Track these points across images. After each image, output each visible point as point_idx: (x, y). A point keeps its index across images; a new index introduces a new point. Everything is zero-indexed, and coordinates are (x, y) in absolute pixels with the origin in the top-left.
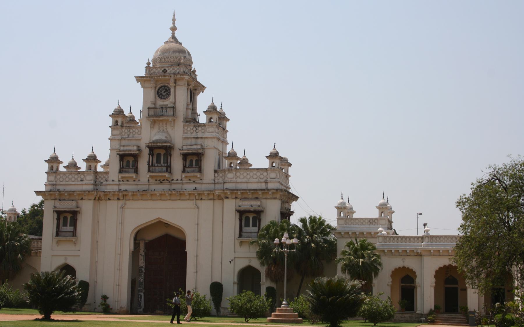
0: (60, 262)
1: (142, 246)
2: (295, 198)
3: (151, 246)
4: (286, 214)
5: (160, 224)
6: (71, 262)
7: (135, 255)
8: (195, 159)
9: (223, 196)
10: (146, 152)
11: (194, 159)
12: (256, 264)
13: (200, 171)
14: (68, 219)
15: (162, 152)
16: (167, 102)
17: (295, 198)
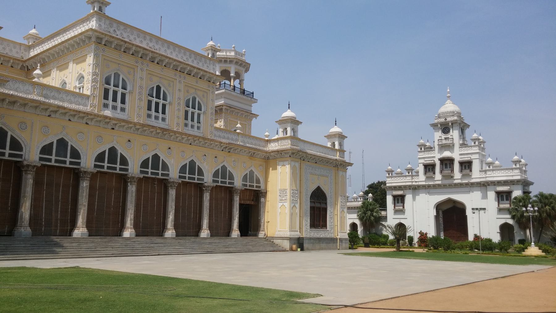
0: (397, 221)
1: (441, 213)
2: (532, 184)
3: (445, 212)
4: (526, 193)
5: (449, 201)
6: (403, 221)
7: (437, 217)
8: (467, 165)
9: (486, 184)
10: (438, 163)
11: (466, 165)
12: (511, 222)
13: (471, 171)
14: (399, 199)
15: (448, 162)
16: (449, 136)
17: (532, 184)
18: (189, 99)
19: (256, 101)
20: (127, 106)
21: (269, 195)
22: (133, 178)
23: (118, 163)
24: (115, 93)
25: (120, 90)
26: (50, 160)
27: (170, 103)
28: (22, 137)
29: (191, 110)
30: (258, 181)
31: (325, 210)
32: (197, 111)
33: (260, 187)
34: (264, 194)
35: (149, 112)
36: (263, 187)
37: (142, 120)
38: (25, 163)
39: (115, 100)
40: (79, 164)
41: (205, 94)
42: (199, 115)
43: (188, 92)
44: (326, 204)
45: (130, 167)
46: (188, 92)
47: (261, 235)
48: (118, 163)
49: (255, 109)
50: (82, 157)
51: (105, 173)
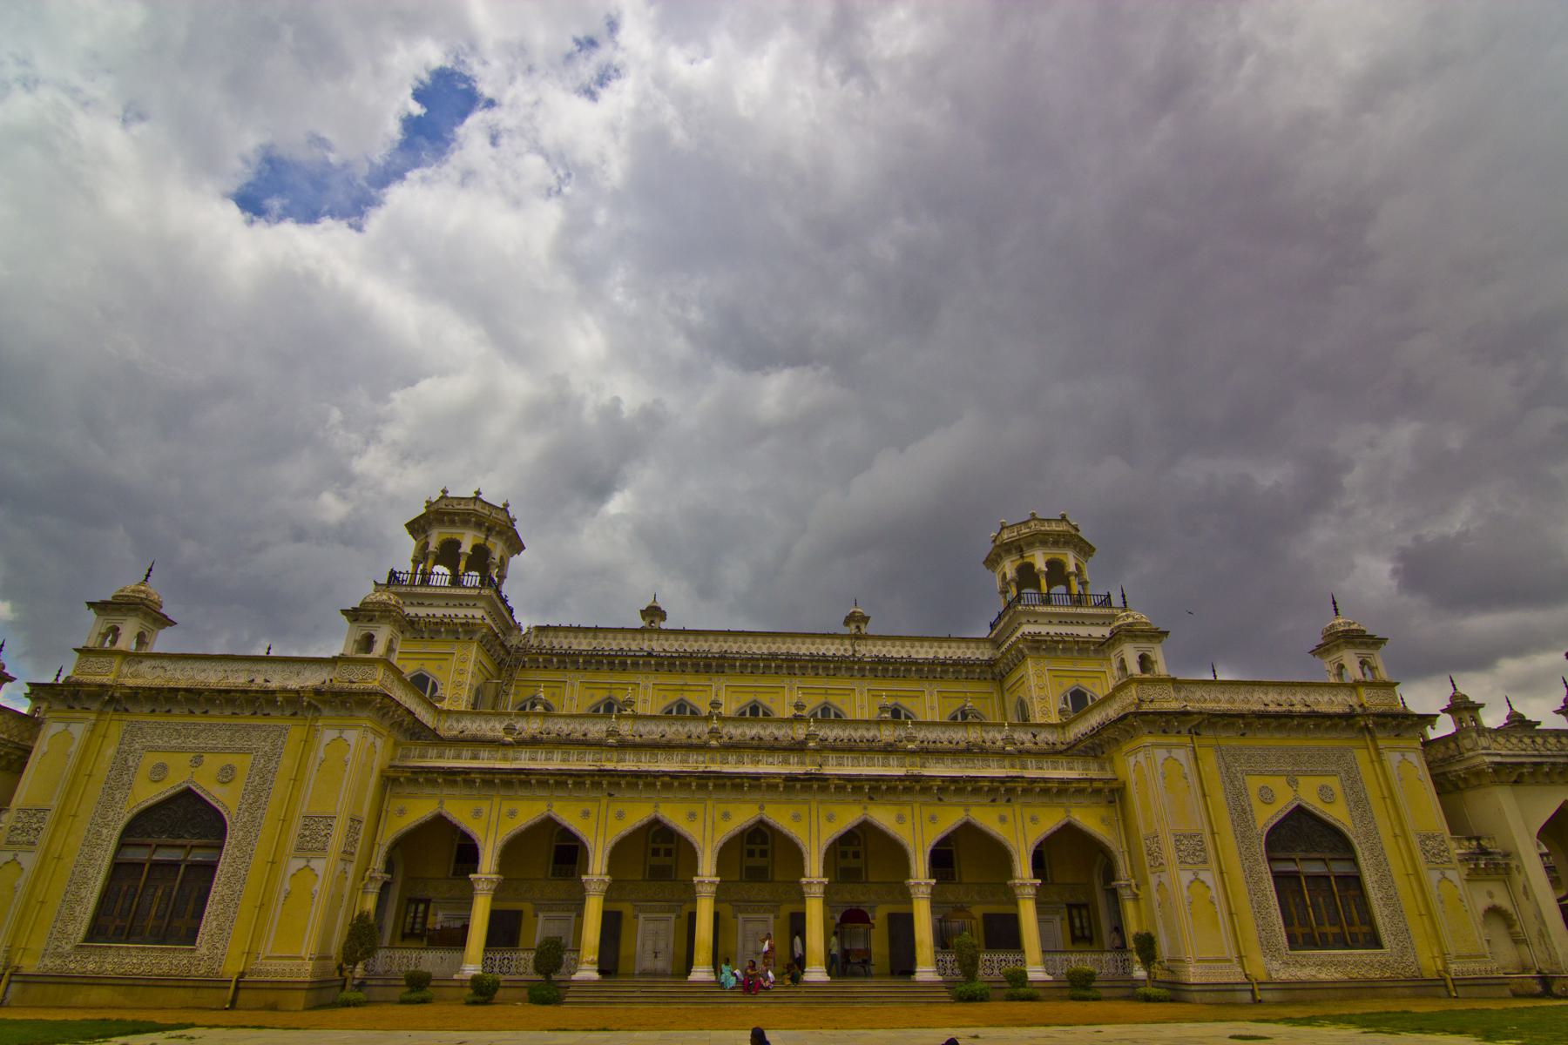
31: (1354, 882)
44: (1353, 860)
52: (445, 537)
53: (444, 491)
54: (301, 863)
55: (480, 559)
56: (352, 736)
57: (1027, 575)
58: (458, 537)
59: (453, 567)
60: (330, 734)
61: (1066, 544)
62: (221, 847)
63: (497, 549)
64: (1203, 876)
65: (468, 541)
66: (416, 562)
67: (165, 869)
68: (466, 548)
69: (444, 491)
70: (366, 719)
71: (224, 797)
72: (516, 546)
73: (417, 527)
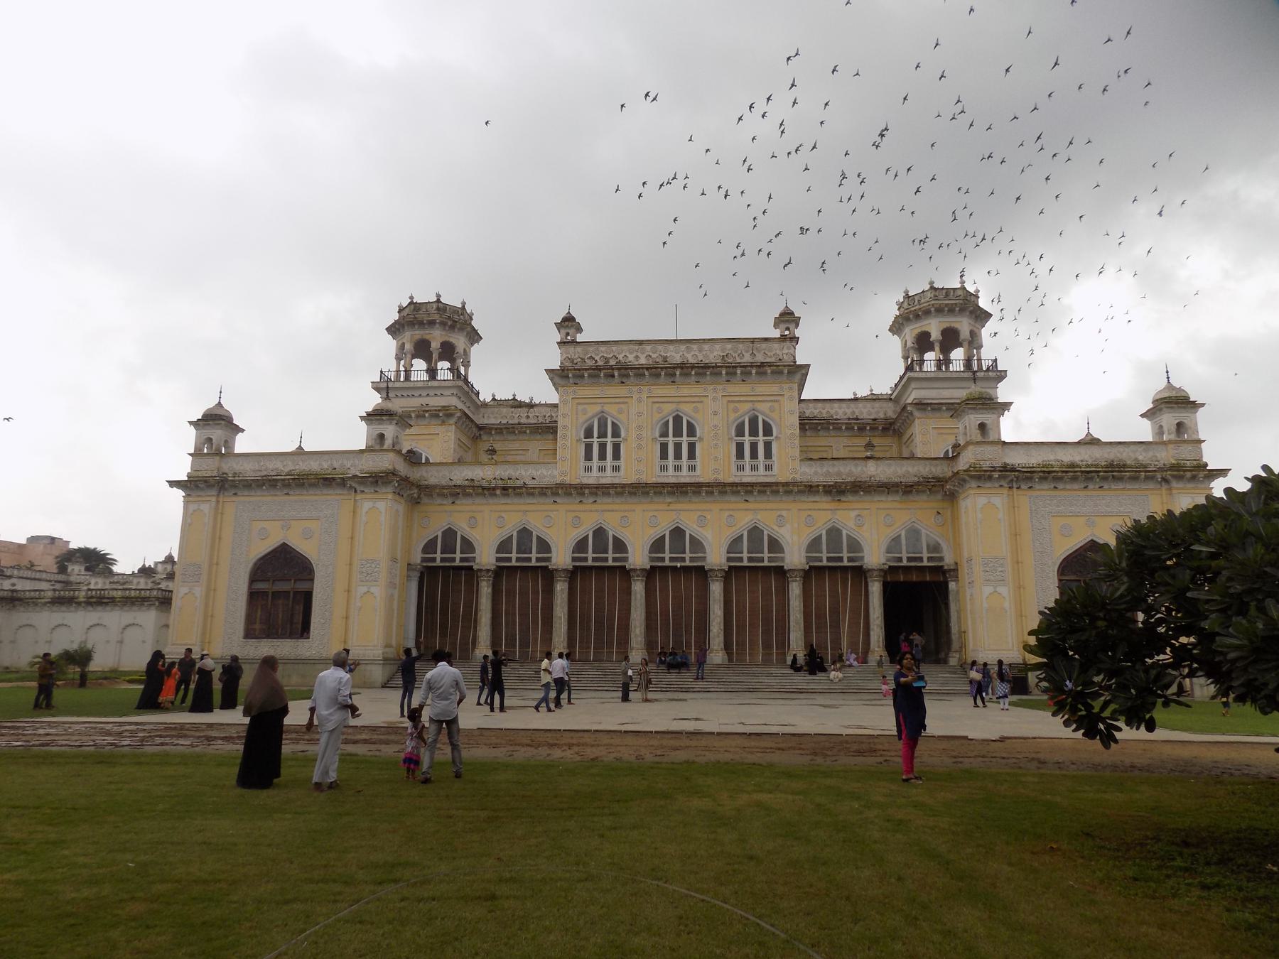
18: (743, 423)
19: (1001, 376)
20: (622, 463)
21: (963, 572)
22: (635, 570)
23: (610, 551)
24: (603, 447)
25: (609, 440)
26: (510, 559)
27: (701, 439)
28: (475, 536)
29: (747, 439)
30: (935, 548)
32: (761, 438)
33: (941, 559)
34: (954, 572)
35: (664, 463)
36: (948, 561)
37: (653, 475)
38: (475, 568)
39: (602, 456)
40: (549, 559)
41: (776, 405)
42: (768, 446)
43: (736, 410)
45: (554, 555)
46: (736, 410)
47: (953, 661)
48: (610, 551)
49: (1003, 392)
50: (553, 549)
51: (591, 568)
52: (418, 337)
53: (411, 298)
54: (364, 589)
55: (448, 351)
56: (381, 505)
57: (923, 343)
58: (427, 337)
59: (428, 359)
60: (367, 505)
61: (962, 310)
62: (312, 580)
63: (459, 341)
64: (1000, 589)
65: (436, 337)
66: (398, 359)
67: (282, 592)
68: (435, 345)
69: (411, 298)
70: (387, 493)
71: (305, 548)
72: (474, 337)
73: (394, 330)
